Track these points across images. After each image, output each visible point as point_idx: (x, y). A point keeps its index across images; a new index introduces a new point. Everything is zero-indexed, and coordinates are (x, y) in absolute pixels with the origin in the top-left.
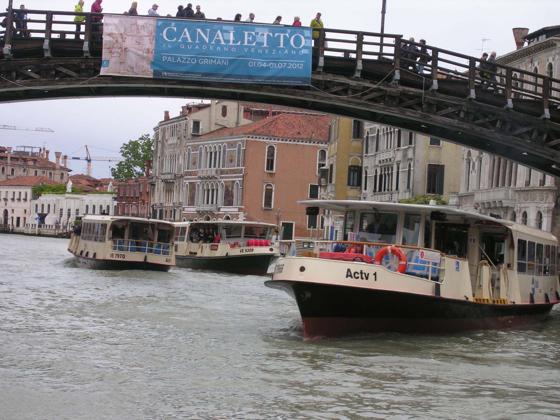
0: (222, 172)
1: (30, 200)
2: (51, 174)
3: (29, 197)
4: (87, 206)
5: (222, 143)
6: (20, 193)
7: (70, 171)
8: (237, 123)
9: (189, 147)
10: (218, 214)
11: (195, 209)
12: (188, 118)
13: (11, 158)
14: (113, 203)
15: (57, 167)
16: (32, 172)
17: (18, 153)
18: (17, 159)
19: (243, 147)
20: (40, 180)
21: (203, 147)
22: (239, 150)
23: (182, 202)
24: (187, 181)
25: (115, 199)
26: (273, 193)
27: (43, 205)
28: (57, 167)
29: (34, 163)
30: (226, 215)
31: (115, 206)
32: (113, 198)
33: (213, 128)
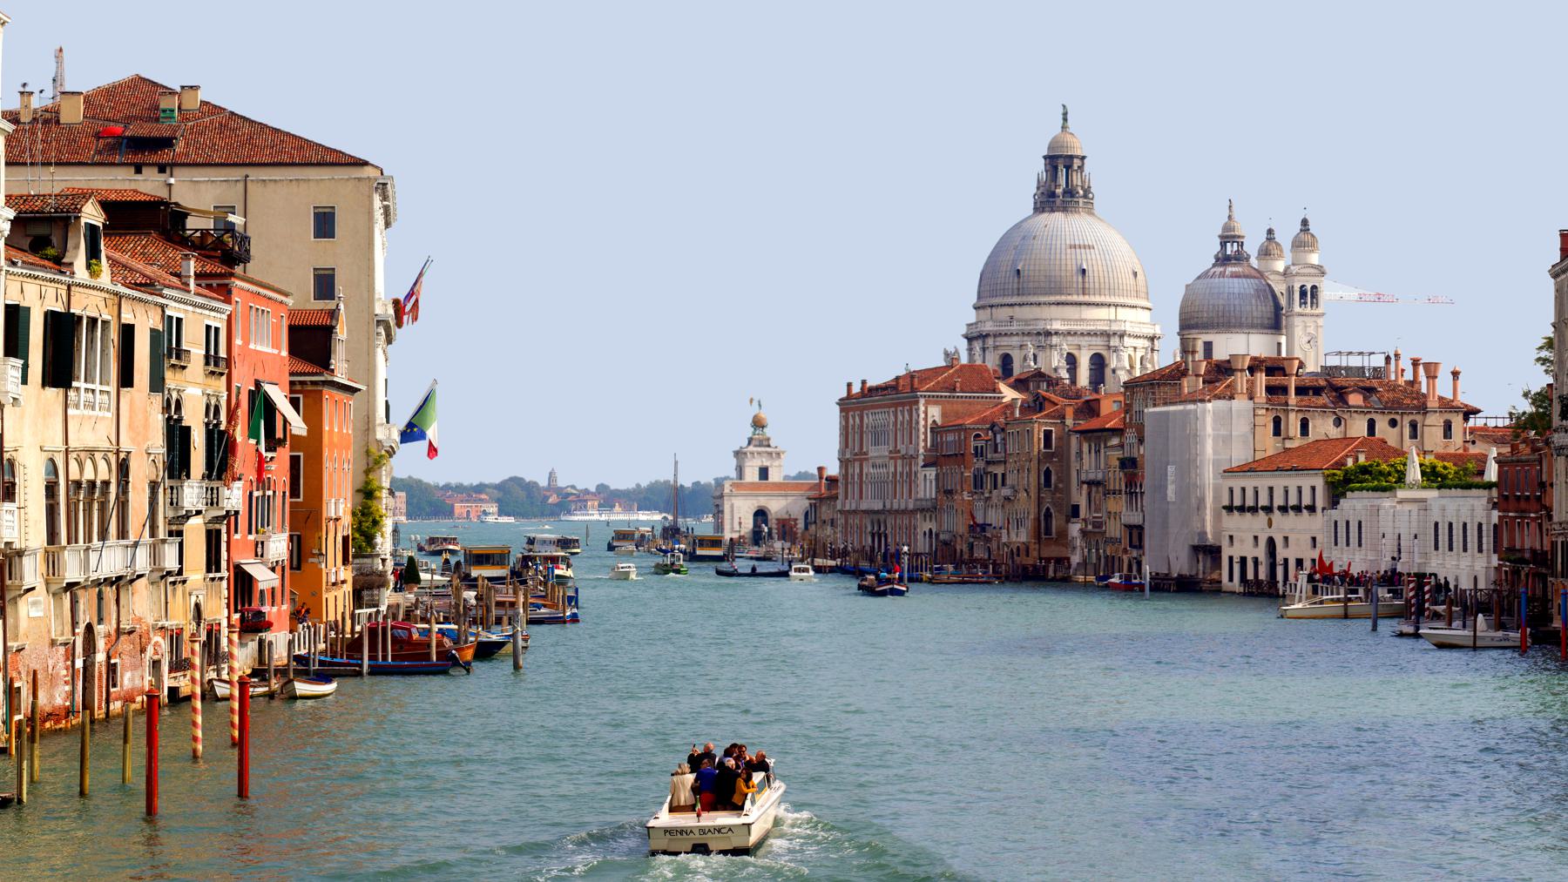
1: (1324, 509)
2: (1414, 426)
3: (1320, 504)
4: (1436, 524)
6: (1300, 490)
7: (1477, 411)
13: (1301, 391)
14: (1489, 517)
15: (1432, 404)
17: (1329, 371)
18: (1318, 391)
20: (1349, 451)
25: (1495, 506)
28: (1429, 405)
29: (1365, 399)
31: (1495, 525)
32: (1490, 500)
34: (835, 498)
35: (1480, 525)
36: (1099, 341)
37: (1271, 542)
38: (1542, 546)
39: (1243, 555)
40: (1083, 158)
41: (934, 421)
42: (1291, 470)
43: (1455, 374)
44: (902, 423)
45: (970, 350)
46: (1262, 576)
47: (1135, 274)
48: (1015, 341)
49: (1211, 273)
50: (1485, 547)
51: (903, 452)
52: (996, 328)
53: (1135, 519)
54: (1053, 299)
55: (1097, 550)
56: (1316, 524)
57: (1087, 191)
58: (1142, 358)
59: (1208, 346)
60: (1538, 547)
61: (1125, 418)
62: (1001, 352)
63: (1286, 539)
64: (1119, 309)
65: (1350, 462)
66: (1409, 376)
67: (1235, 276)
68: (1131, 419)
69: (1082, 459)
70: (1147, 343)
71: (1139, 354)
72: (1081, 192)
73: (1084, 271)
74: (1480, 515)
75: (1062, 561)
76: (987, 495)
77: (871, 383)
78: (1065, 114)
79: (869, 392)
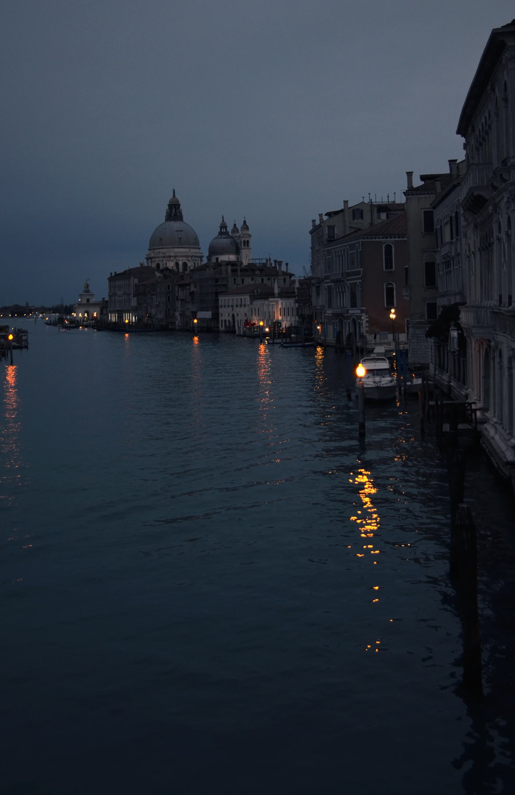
0: (348, 274)
5: (346, 246)
6: (241, 299)
8: (371, 224)
9: (325, 252)
10: (347, 316)
11: (330, 312)
12: (323, 225)
14: (295, 305)
15: (280, 273)
16: (259, 280)
18: (247, 270)
19: (360, 249)
21: (334, 251)
22: (357, 251)
23: (324, 305)
24: (326, 285)
25: (296, 302)
26: (395, 291)
27: (255, 309)
29: (260, 272)
30: (353, 317)
31: (297, 308)
32: (295, 300)
33: (348, 232)
34: (107, 307)
35: (293, 308)
36: (184, 259)
37: (233, 315)
38: (310, 313)
39: (225, 319)
40: (180, 205)
41: (136, 283)
42: (238, 294)
43: (287, 264)
44: (127, 284)
45: (147, 262)
46: (232, 325)
47: (195, 238)
48: (161, 259)
49: (217, 238)
50: (294, 314)
51: (127, 293)
52: (155, 256)
53: (195, 310)
54: (171, 246)
55: (184, 320)
56: (246, 310)
57: (181, 214)
58: (198, 263)
59: (217, 259)
60: (309, 314)
61: (191, 280)
62: (156, 263)
63: (238, 314)
64: (191, 249)
65: (256, 291)
66: (273, 265)
67: (224, 238)
68: (192, 280)
69: (179, 293)
70: (200, 259)
71: (197, 262)
72: (179, 215)
73: (180, 238)
74: (293, 305)
75: (173, 323)
76: (151, 304)
77: (117, 273)
78: (174, 192)
79: (117, 275)
